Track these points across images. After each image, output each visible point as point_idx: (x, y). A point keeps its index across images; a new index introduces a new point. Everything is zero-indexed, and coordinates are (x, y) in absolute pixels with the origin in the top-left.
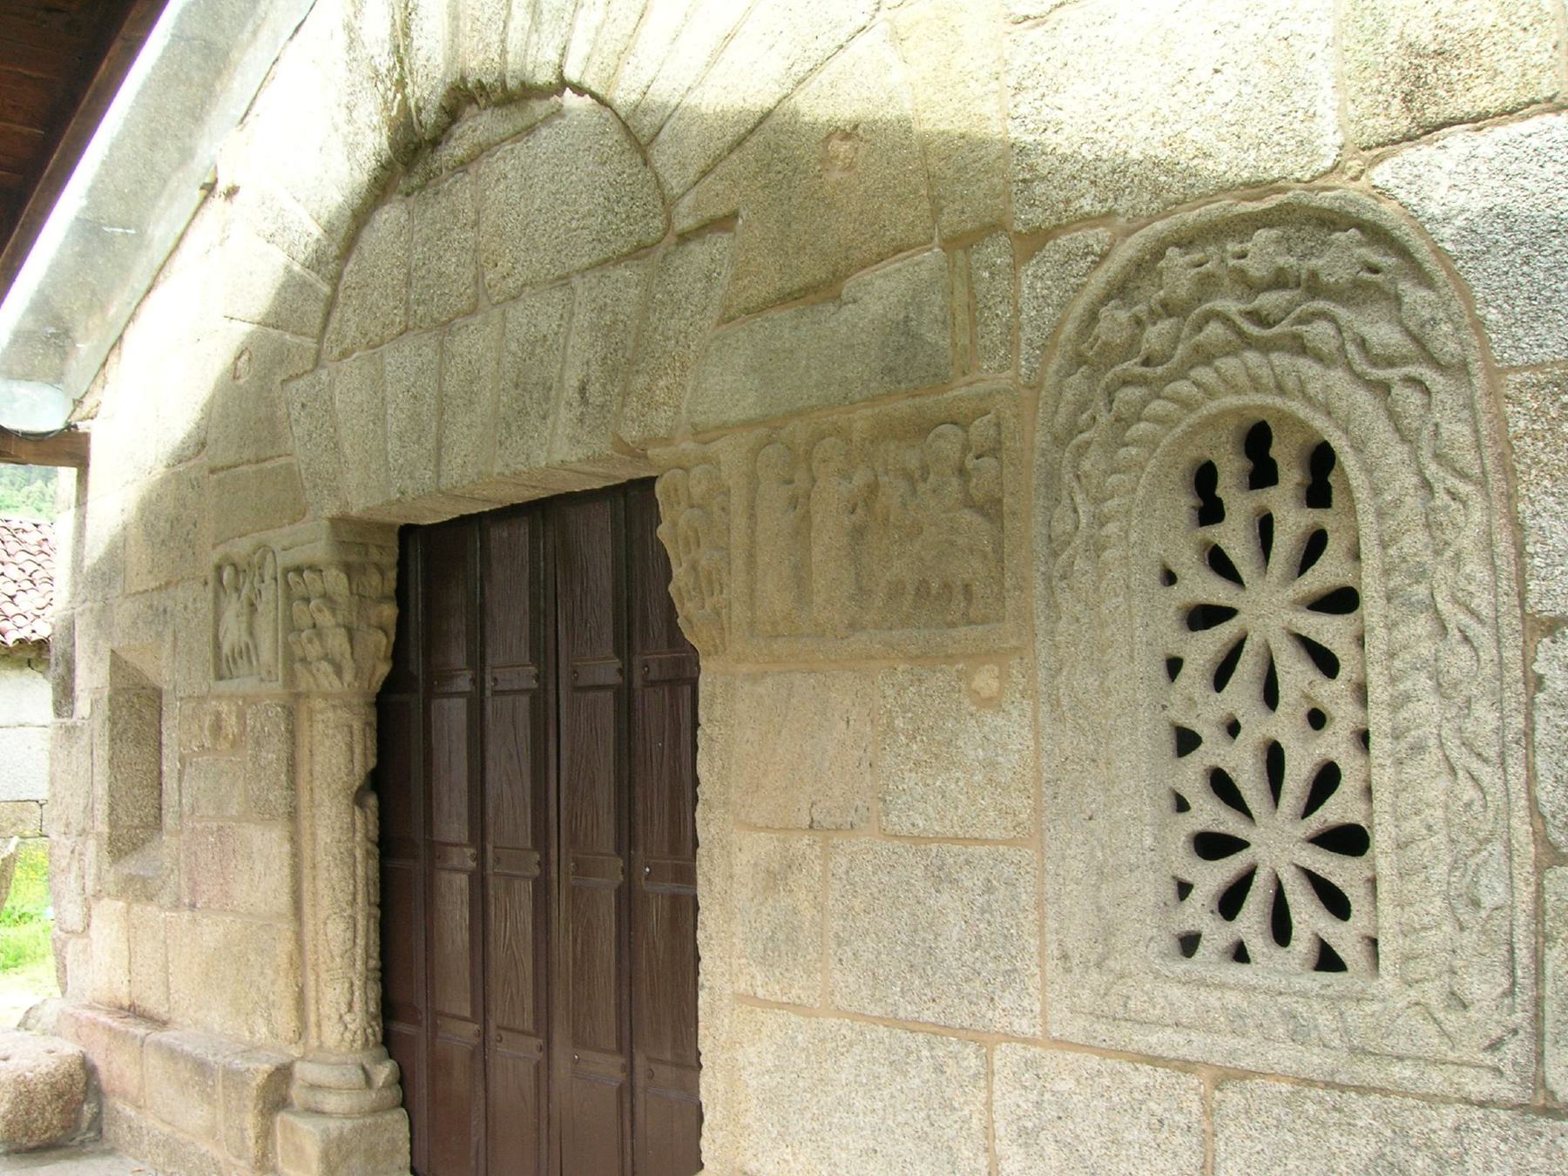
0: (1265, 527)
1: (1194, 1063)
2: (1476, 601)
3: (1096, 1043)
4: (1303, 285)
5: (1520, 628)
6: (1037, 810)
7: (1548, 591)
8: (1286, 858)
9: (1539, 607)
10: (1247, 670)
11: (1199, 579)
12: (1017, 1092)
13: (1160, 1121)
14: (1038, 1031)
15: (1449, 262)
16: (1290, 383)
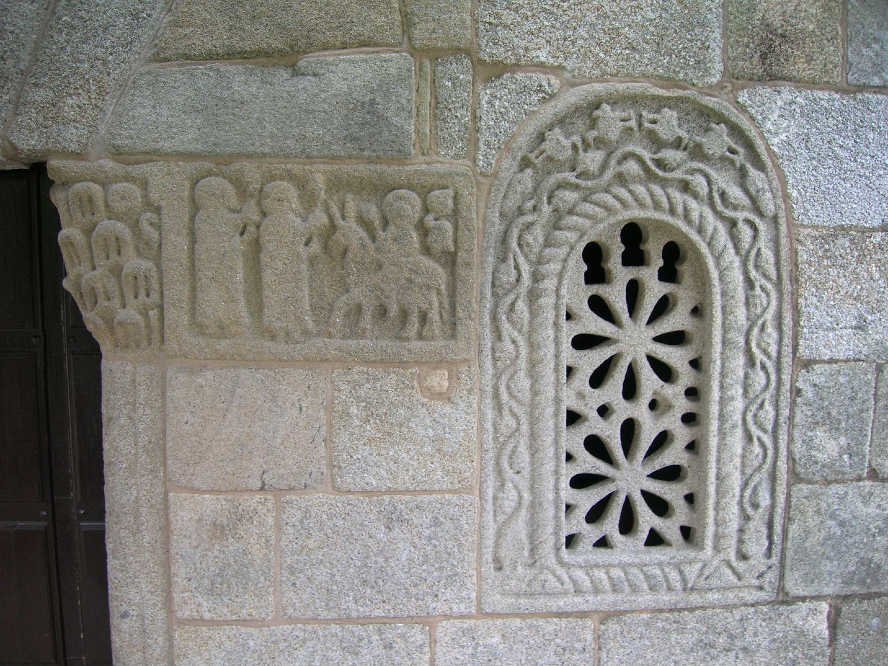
0: (634, 291)
1: (588, 612)
2: (771, 348)
10: (618, 377)
12: (456, 650)
13: (564, 649)
14: (473, 610)
15: (774, 158)
16: (680, 209)
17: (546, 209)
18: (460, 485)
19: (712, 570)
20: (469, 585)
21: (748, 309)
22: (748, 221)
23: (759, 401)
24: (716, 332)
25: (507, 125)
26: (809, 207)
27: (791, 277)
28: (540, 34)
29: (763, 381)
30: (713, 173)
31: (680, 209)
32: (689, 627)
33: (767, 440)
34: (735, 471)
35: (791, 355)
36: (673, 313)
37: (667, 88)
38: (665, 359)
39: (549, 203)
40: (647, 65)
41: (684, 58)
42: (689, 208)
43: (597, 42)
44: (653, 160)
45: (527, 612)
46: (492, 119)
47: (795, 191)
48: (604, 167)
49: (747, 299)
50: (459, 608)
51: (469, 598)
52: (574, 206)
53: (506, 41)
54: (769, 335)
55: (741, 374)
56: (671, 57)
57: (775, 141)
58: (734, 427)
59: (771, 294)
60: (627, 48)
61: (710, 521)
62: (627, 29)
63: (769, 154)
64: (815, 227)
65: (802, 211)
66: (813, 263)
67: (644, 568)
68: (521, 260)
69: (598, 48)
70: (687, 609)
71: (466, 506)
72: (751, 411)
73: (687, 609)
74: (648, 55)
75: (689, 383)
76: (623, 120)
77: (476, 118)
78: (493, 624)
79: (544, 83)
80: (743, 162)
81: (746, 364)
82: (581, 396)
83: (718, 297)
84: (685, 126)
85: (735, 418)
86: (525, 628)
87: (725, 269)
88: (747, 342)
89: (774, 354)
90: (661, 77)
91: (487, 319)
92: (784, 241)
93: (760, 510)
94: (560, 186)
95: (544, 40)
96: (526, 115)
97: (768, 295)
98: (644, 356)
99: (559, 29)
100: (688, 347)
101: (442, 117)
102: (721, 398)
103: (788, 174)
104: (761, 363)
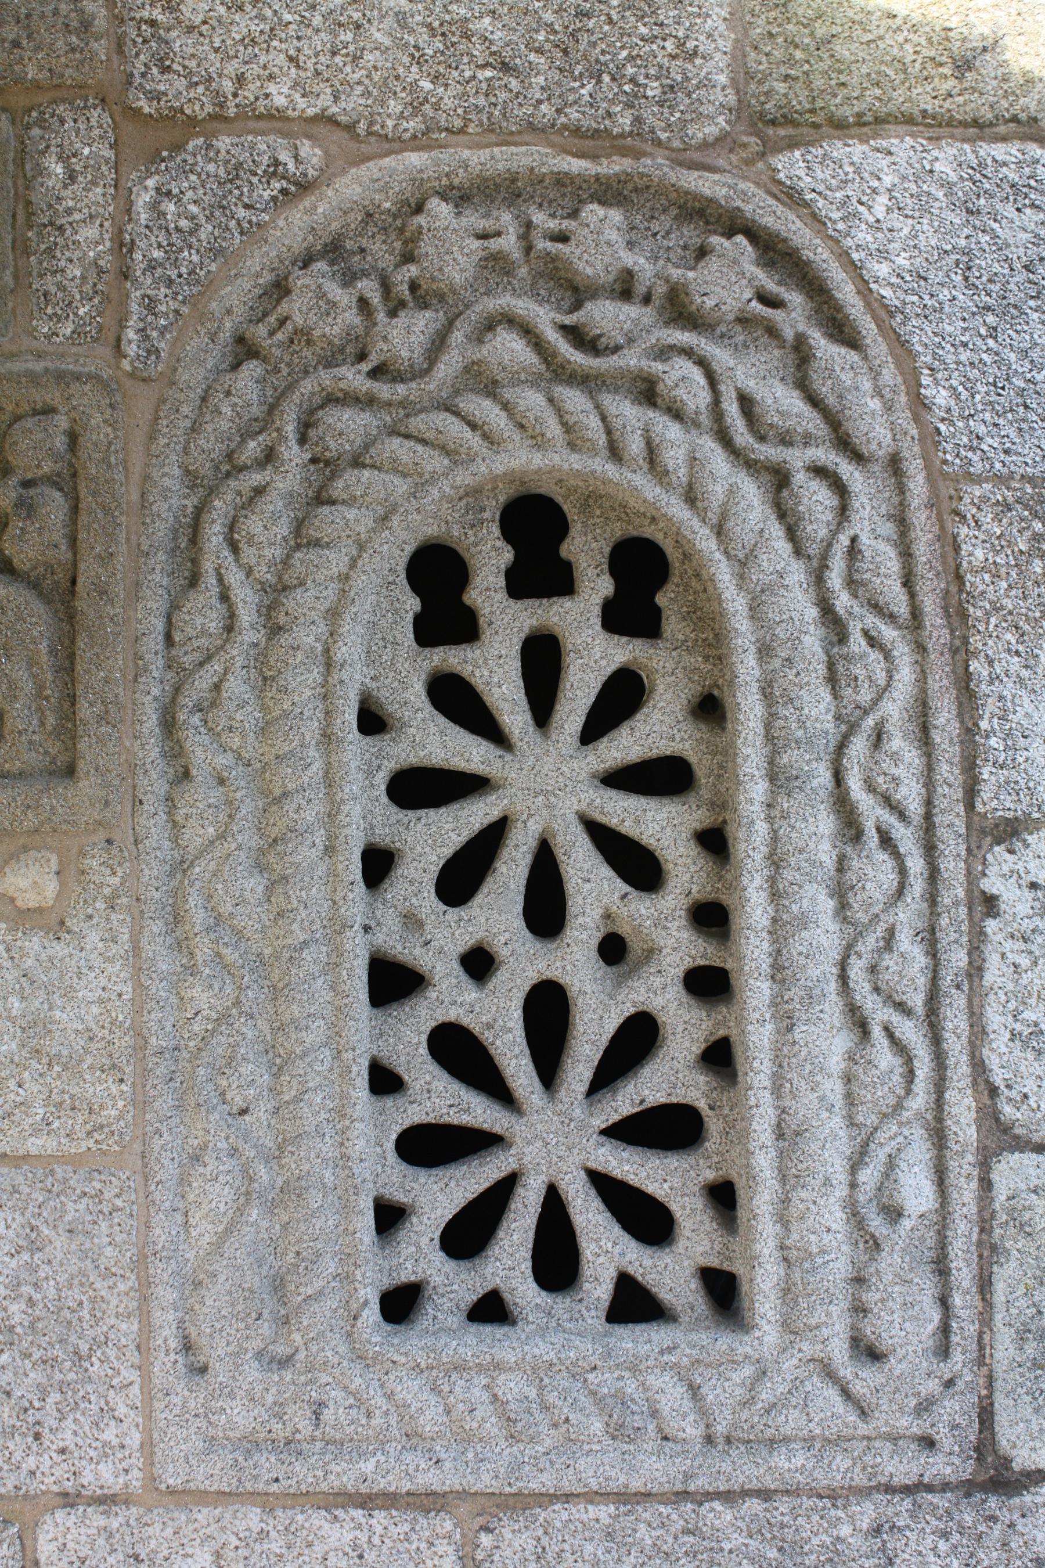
1: (444, 1495)
2: (903, 790)
3: (261, 1487)
4: (656, 301)
5: (963, 831)
6: (141, 1103)
7: (1007, 783)
8: (576, 1158)
9: (994, 804)
11: (433, 729)
16: (635, 446)
17: (293, 454)
18: (91, 1143)
19: (782, 1389)
20: (122, 1410)
21: (836, 695)
22: (819, 471)
23: (880, 929)
24: (749, 750)
25: (195, 258)
26: (982, 430)
27: (945, 609)
28: (275, 43)
29: (889, 878)
30: (720, 355)
31: (635, 446)
32: (727, 1546)
33: (911, 1032)
34: (825, 1114)
35: (961, 808)
36: (645, 710)
37: (594, 157)
38: (628, 828)
39: (303, 440)
40: (540, 102)
41: (633, 80)
42: (657, 440)
43: (412, 56)
44: (564, 328)
45: (274, 1488)
46: (160, 246)
47: (944, 393)
48: (438, 344)
49: (831, 666)
50: (97, 1476)
51: (123, 1447)
52: (366, 447)
53: (193, 64)
54: (895, 758)
55: (828, 860)
56: (599, 81)
57: (883, 270)
58: (810, 998)
59: (895, 653)
60: (486, 65)
61: (766, 1252)
62: (487, 20)
63: (868, 305)
64: (1001, 480)
65: (965, 439)
66: (1003, 570)
67: (591, 1377)
68: (235, 577)
69: (415, 69)
70: (718, 1495)
71: (107, 1195)
72: (860, 957)
73: (718, 1495)
74: (541, 80)
75: (695, 888)
76: (483, 236)
77: (123, 247)
78: (188, 1521)
79: (284, 157)
80: (801, 327)
81: (840, 834)
82: (412, 921)
83: (751, 660)
84: (648, 244)
85: (814, 972)
86: (273, 1534)
87: (763, 591)
88: (838, 778)
89: (915, 807)
90: (576, 131)
91: (151, 721)
92: (920, 518)
93: (907, 1224)
94: (331, 400)
95: (282, 56)
96: (242, 233)
97: (887, 655)
98: (572, 818)
99: (318, 31)
100: (692, 799)
101: (43, 247)
102: (775, 920)
103: (920, 349)
104: (879, 829)
